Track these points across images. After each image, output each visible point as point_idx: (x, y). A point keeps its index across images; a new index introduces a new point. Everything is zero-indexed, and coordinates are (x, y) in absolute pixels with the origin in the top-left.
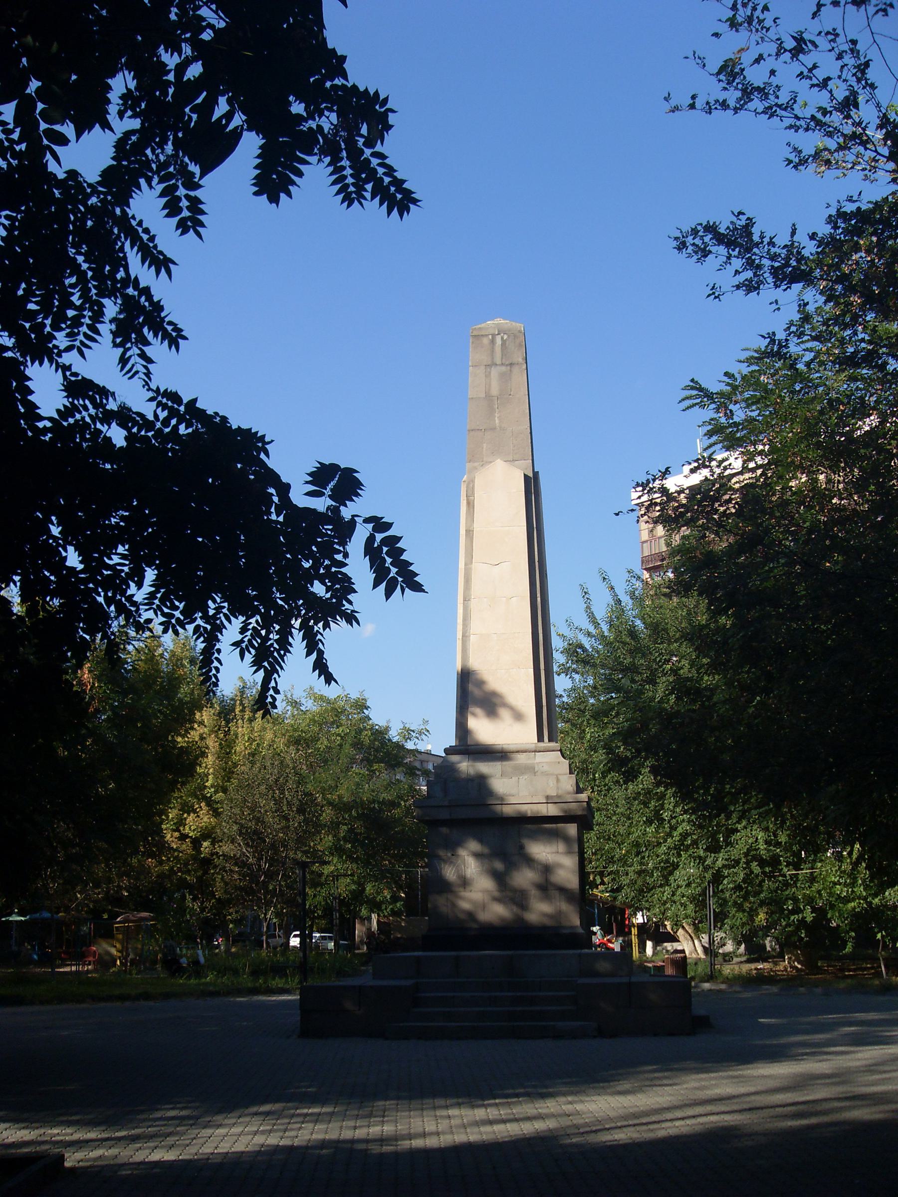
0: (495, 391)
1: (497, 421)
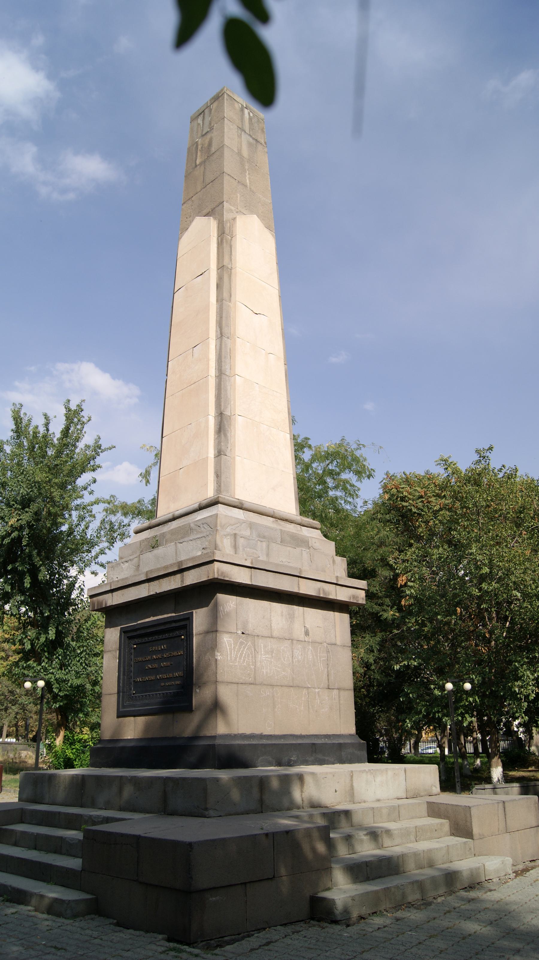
0: (245, 153)
1: (248, 181)
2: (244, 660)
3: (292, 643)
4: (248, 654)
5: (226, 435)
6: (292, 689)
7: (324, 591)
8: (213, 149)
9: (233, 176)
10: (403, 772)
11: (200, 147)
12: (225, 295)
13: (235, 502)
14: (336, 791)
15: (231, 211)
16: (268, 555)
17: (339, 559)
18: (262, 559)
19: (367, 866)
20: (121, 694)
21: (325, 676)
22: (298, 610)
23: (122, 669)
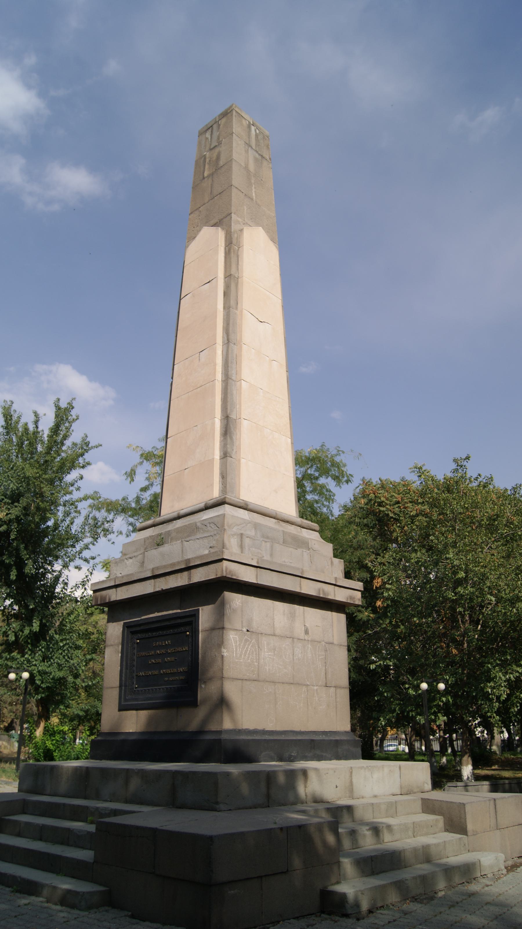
0: (252, 167)
1: (254, 195)
2: (248, 658)
3: (293, 641)
4: (253, 652)
5: (231, 438)
6: (292, 686)
7: (323, 591)
8: (221, 163)
9: (240, 189)
10: (398, 769)
11: (207, 160)
12: (232, 303)
13: (240, 502)
14: (337, 787)
15: (238, 222)
16: (271, 555)
17: (336, 561)
18: (266, 559)
19: (372, 861)
20: (123, 688)
21: (323, 673)
22: (299, 609)
23: (124, 663)
